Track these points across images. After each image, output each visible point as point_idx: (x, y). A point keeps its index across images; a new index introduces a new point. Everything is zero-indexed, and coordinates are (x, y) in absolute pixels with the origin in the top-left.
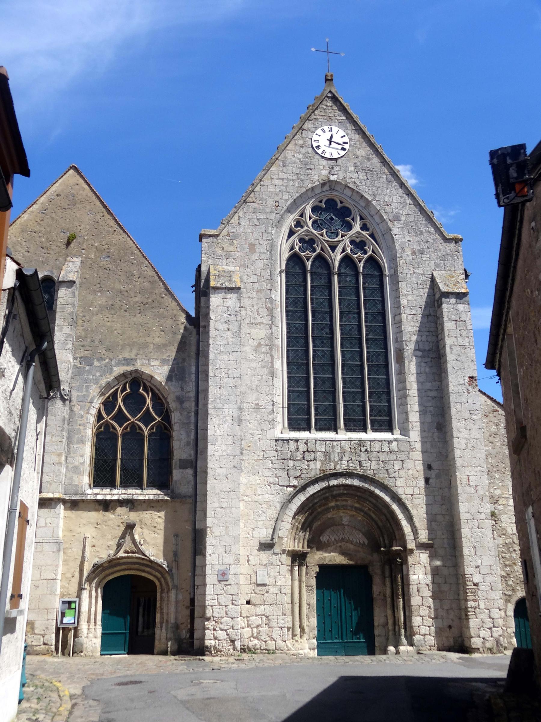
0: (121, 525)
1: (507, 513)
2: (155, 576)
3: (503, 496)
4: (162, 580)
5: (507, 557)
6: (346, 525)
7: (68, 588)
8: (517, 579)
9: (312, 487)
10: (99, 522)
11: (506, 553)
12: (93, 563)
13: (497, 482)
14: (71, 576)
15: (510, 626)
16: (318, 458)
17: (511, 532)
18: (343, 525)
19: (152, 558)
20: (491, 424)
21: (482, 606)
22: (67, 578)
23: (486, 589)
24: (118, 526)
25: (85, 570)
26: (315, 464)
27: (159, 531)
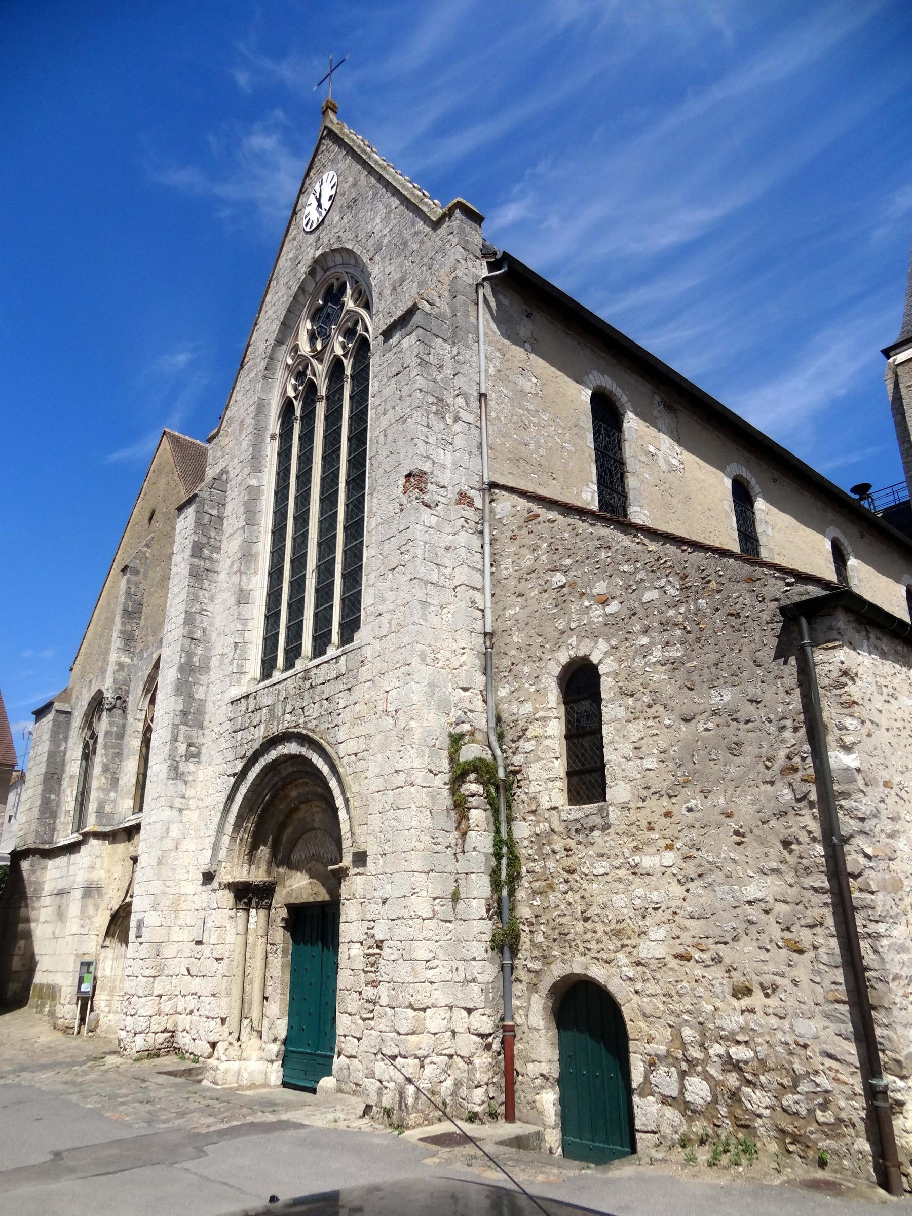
1: (542, 756)
3: (537, 716)
5: (538, 869)
6: (319, 829)
8: (553, 929)
9: (253, 769)
11: (535, 860)
13: (527, 685)
15: (534, 1056)
16: (264, 719)
17: (548, 805)
18: (314, 829)
20: (524, 551)
21: (384, 1001)
23: (393, 957)
26: (260, 729)
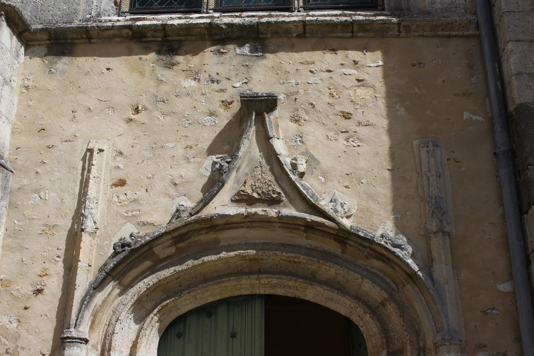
0: (221, 110)
2: (358, 298)
4: (391, 309)
7: (17, 337)
10: (144, 101)
12: (115, 240)
14: (29, 290)
19: (347, 223)
22: (16, 298)
24: (211, 114)
25: (82, 265)
27: (363, 131)
